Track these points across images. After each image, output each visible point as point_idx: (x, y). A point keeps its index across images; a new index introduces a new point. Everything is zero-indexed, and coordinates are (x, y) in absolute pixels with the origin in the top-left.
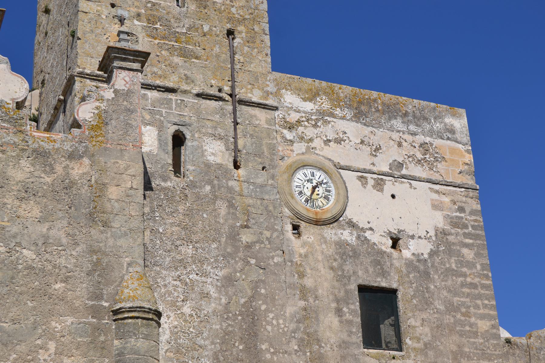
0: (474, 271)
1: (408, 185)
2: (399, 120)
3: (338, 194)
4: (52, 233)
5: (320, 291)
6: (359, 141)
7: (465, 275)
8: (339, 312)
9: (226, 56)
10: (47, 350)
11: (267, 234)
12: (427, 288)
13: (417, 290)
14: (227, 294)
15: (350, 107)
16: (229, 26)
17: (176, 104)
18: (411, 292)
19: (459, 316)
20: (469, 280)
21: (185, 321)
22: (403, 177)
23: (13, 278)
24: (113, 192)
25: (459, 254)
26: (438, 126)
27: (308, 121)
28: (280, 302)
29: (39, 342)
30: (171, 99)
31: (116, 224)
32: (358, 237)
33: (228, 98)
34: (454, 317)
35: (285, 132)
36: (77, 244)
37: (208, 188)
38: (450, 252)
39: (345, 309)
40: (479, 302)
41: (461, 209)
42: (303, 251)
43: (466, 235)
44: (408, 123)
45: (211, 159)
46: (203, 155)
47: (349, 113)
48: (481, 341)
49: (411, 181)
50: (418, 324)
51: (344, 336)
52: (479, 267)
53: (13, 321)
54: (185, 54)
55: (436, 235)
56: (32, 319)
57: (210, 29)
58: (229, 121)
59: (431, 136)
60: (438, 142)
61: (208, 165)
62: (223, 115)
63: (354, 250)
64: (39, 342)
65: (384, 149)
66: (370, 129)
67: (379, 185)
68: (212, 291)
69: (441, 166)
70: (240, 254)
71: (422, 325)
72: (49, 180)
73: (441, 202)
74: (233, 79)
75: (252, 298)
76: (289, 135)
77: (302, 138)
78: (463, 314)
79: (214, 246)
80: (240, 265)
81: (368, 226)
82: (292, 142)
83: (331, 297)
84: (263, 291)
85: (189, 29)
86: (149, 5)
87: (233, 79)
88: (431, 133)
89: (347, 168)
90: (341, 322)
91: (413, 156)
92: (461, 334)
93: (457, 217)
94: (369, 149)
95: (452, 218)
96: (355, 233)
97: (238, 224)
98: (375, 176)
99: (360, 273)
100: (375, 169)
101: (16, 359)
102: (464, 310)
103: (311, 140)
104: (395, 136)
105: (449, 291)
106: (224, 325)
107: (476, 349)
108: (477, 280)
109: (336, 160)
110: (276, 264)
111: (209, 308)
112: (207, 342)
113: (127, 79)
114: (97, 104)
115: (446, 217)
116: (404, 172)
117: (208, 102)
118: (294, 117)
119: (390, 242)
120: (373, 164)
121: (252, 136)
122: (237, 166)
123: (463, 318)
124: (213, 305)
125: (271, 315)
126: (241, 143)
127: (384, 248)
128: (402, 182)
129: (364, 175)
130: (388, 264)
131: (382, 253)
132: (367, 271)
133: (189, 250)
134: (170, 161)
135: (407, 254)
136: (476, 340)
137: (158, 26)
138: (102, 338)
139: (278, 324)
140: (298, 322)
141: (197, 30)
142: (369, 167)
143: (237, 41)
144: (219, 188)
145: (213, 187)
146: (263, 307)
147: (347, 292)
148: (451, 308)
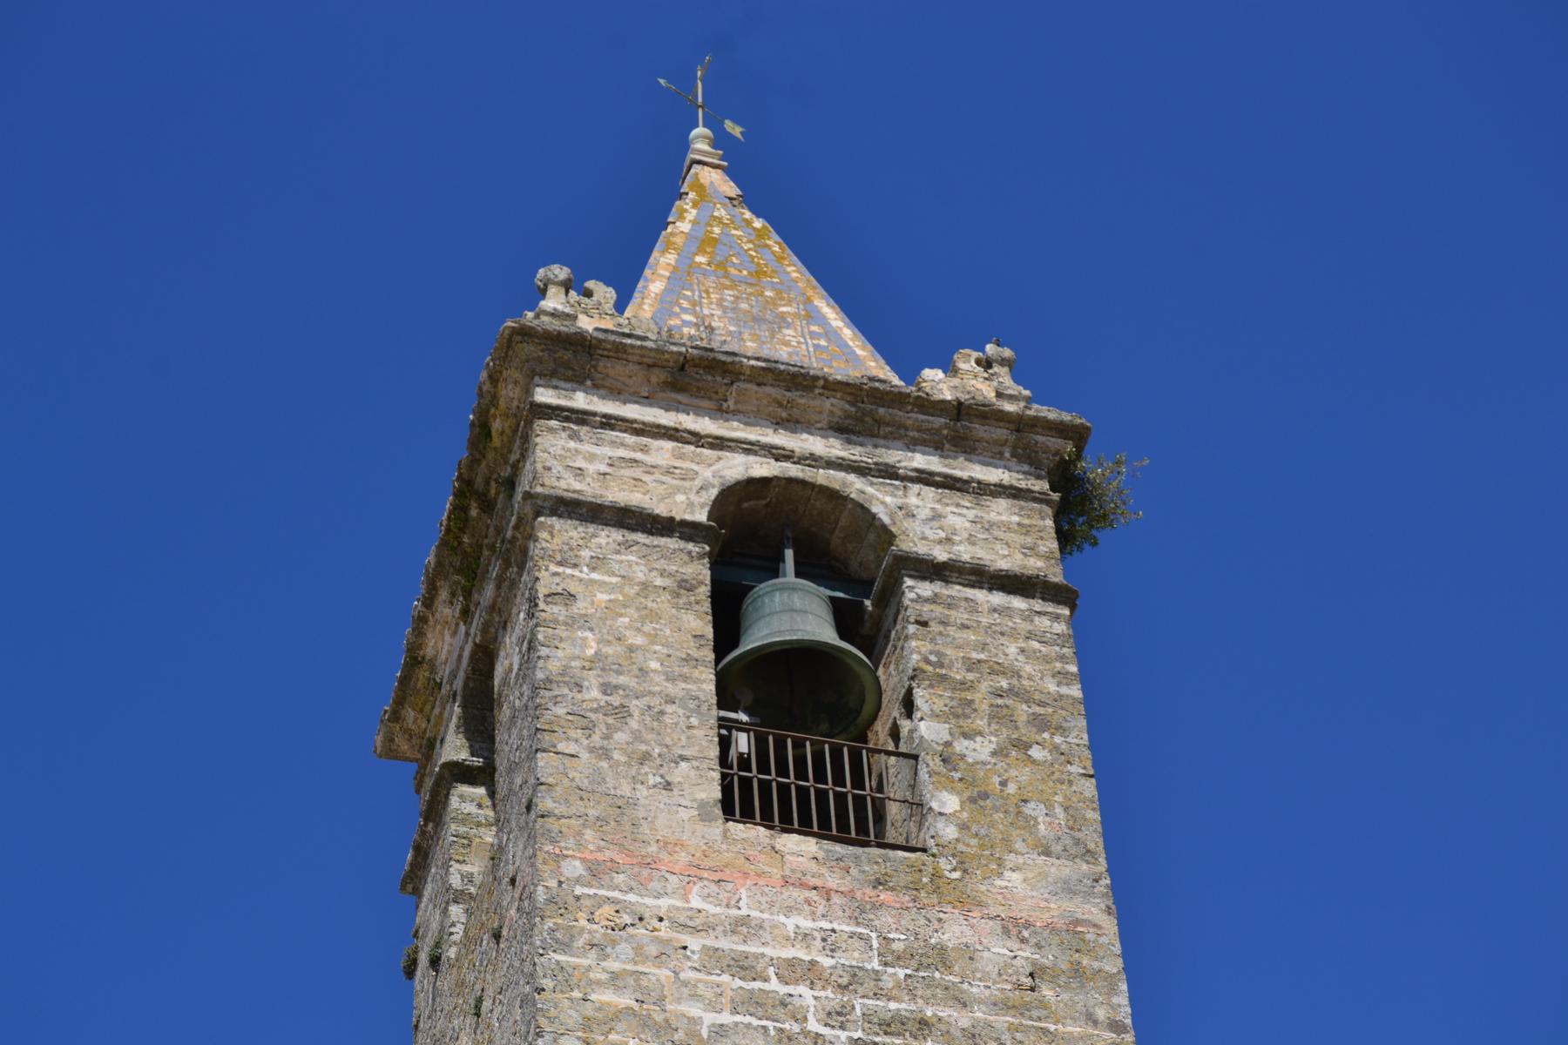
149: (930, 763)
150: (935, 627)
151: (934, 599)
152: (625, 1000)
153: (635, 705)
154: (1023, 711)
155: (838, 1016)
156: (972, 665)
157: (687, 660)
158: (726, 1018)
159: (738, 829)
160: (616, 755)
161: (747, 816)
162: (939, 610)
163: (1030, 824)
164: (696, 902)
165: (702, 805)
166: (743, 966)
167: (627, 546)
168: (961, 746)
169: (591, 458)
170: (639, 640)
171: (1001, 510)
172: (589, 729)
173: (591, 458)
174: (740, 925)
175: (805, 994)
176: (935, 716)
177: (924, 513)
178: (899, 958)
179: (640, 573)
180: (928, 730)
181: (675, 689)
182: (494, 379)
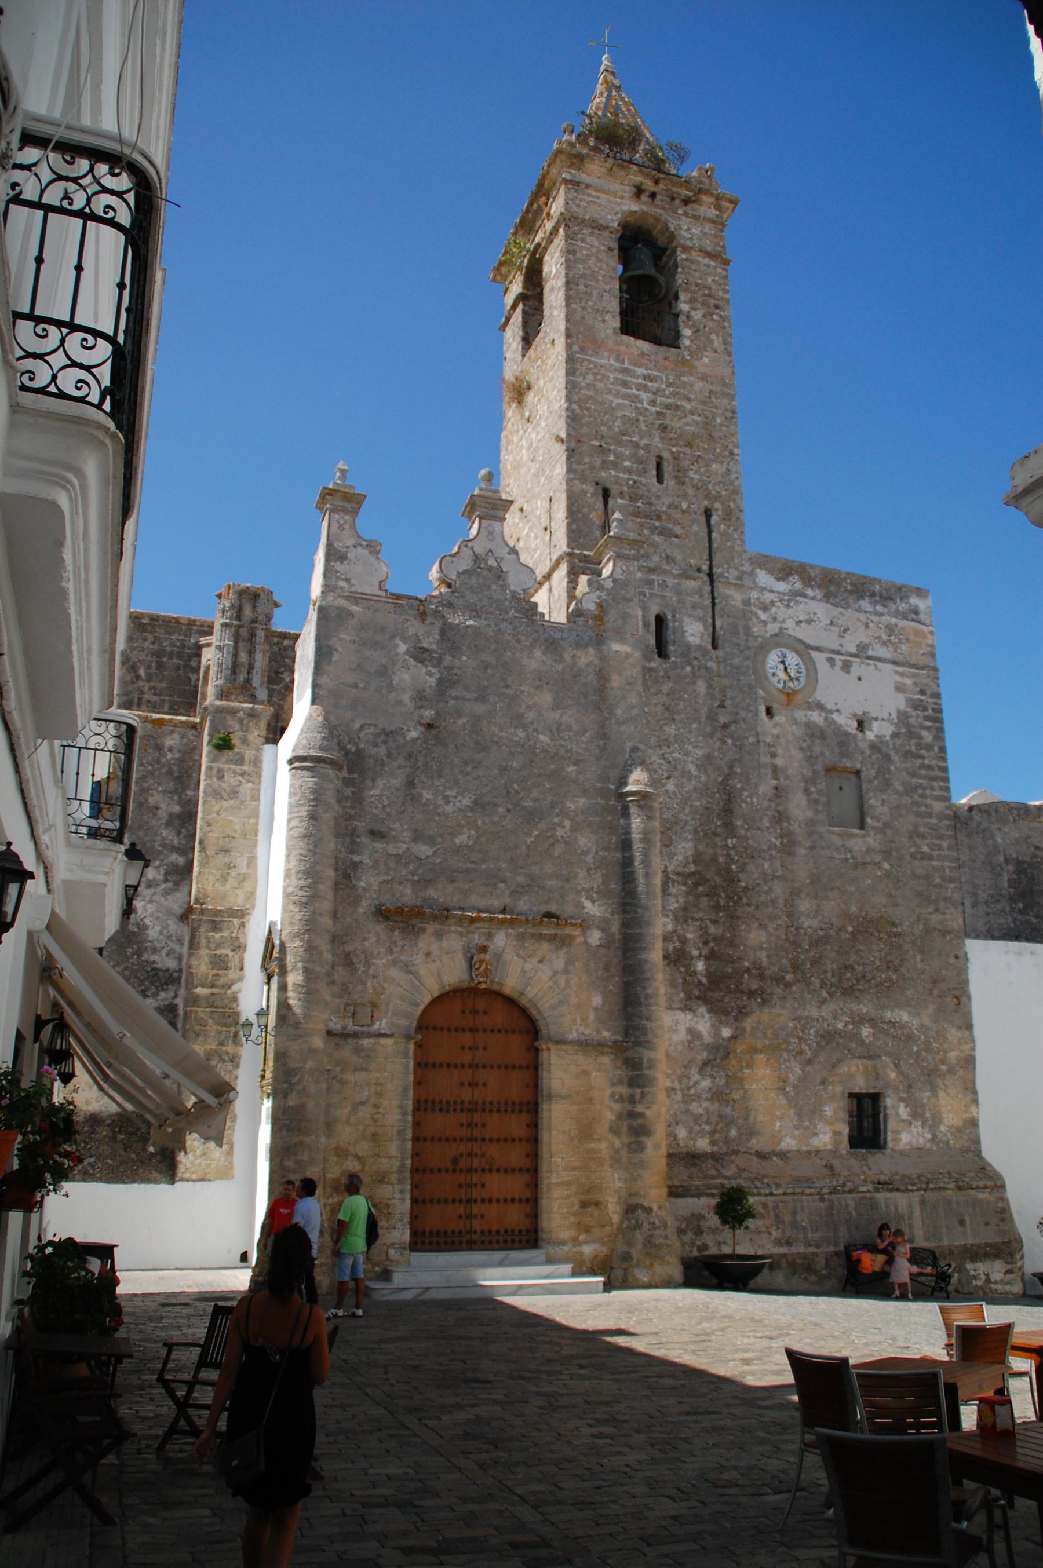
0: (931, 753)
1: (873, 667)
2: (867, 599)
3: (808, 675)
4: (565, 718)
5: (790, 771)
6: (828, 622)
7: (923, 757)
8: (807, 791)
9: (704, 533)
10: (564, 827)
11: (743, 714)
12: (889, 769)
13: (879, 771)
14: (706, 770)
15: (819, 586)
16: (706, 502)
17: (659, 585)
18: (873, 773)
19: (916, 798)
20: (926, 762)
21: (669, 797)
22: (869, 658)
23: (532, 761)
24: (616, 681)
25: (921, 738)
26: (903, 606)
27: (781, 601)
28: (754, 781)
29: (556, 820)
30: (653, 580)
31: (619, 712)
32: (826, 719)
33: (706, 578)
34: (912, 797)
35: (760, 613)
36: (585, 731)
37: (689, 668)
38: (911, 735)
39: (813, 789)
40: (935, 784)
41: (922, 692)
42: (775, 732)
43: (927, 718)
44: (874, 603)
45: (691, 639)
46: (684, 637)
47: (818, 593)
48: (935, 821)
49: (877, 663)
50: (878, 804)
51: (810, 814)
52: (936, 749)
53: (535, 800)
54: (664, 532)
55: (898, 717)
56: (550, 799)
57: (689, 507)
58: (708, 602)
59: (896, 617)
60: (903, 623)
61: (688, 646)
62: (701, 596)
63: (822, 731)
64: (556, 820)
65: (852, 630)
66: (840, 609)
67: (846, 667)
68: (692, 768)
69: (904, 648)
70: (718, 735)
71: (882, 805)
72: (559, 668)
73: (904, 684)
74: (710, 559)
75: (729, 776)
76: (763, 616)
77: (775, 619)
78: (922, 796)
79: (694, 726)
80: (718, 744)
81: (834, 708)
82: (765, 623)
83: (800, 778)
84: (739, 770)
85: (669, 506)
86: (631, 482)
87: (710, 559)
88: (897, 614)
89: (818, 649)
90: (808, 800)
91: (878, 638)
92: (917, 814)
93: (918, 699)
94: (837, 629)
95: (913, 700)
96: (823, 714)
97: (716, 705)
98: (843, 658)
99: (827, 754)
100: (843, 650)
101: (537, 836)
102: (920, 791)
103: (784, 621)
104: (863, 617)
105: (909, 773)
106: (704, 802)
107: (931, 829)
108: (934, 762)
109: (808, 641)
110: (751, 744)
111: (689, 787)
112: (688, 818)
113: (624, 568)
114: (598, 593)
115: (908, 700)
116: (870, 653)
117: (688, 582)
118: (768, 597)
119: (855, 724)
120: (841, 645)
121: (729, 616)
122: (715, 646)
123: (920, 799)
124: (694, 783)
125: (746, 793)
126: (718, 623)
127: (850, 730)
128: (868, 664)
129: (833, 656)
130: (853, 745)
131: (847, 734)
132: (833, 752)
133: (671, 730)
134: (652, 641)
135: (870, 735)
136: (931, 821)
137: (639, 504)
138: (610, 818)
139: (752, 803)
140: (770, 800)
141: (676, 507)
142: (837, 648)
143: (714, 519)
144: (699, 668)
145: (693, 668)
146: (739, 786)
147: (815, 772)
148: (909, 790)
149: (682, 318)
150: (687, 270)
151: (687, 260)
152: (590, 393)
153: (595, 292)
154: (713, 302)
155: (653, 403)
156: (697, 285)
157: (610, 277)
158: (620, 401)
159: (625, 338)
160: (589, 310)
161: (627, 334)
162: (688, 264)
163: (711, 342)
164: (612, 362)
165: (614, 329)
166: (625, 384)
167: (591, 234)
168: (693, 313)
169: (581, 200)
170: (596, 269)
171: (709, 228)
172: (581, 299)
173: (581, 200)
174: (626, 371)
175: (643, 395)
176: (685, 302)
177: (685, 227)
178: (670, 385)
179: (596, 243)
180: (684, 307)
181: (607, 287)
182: (549, 166)
